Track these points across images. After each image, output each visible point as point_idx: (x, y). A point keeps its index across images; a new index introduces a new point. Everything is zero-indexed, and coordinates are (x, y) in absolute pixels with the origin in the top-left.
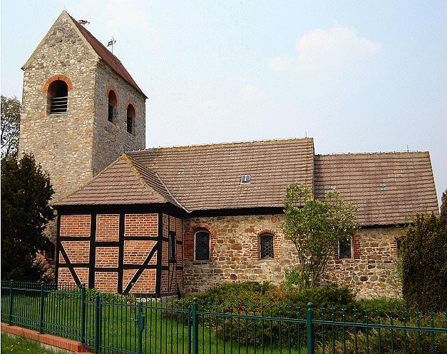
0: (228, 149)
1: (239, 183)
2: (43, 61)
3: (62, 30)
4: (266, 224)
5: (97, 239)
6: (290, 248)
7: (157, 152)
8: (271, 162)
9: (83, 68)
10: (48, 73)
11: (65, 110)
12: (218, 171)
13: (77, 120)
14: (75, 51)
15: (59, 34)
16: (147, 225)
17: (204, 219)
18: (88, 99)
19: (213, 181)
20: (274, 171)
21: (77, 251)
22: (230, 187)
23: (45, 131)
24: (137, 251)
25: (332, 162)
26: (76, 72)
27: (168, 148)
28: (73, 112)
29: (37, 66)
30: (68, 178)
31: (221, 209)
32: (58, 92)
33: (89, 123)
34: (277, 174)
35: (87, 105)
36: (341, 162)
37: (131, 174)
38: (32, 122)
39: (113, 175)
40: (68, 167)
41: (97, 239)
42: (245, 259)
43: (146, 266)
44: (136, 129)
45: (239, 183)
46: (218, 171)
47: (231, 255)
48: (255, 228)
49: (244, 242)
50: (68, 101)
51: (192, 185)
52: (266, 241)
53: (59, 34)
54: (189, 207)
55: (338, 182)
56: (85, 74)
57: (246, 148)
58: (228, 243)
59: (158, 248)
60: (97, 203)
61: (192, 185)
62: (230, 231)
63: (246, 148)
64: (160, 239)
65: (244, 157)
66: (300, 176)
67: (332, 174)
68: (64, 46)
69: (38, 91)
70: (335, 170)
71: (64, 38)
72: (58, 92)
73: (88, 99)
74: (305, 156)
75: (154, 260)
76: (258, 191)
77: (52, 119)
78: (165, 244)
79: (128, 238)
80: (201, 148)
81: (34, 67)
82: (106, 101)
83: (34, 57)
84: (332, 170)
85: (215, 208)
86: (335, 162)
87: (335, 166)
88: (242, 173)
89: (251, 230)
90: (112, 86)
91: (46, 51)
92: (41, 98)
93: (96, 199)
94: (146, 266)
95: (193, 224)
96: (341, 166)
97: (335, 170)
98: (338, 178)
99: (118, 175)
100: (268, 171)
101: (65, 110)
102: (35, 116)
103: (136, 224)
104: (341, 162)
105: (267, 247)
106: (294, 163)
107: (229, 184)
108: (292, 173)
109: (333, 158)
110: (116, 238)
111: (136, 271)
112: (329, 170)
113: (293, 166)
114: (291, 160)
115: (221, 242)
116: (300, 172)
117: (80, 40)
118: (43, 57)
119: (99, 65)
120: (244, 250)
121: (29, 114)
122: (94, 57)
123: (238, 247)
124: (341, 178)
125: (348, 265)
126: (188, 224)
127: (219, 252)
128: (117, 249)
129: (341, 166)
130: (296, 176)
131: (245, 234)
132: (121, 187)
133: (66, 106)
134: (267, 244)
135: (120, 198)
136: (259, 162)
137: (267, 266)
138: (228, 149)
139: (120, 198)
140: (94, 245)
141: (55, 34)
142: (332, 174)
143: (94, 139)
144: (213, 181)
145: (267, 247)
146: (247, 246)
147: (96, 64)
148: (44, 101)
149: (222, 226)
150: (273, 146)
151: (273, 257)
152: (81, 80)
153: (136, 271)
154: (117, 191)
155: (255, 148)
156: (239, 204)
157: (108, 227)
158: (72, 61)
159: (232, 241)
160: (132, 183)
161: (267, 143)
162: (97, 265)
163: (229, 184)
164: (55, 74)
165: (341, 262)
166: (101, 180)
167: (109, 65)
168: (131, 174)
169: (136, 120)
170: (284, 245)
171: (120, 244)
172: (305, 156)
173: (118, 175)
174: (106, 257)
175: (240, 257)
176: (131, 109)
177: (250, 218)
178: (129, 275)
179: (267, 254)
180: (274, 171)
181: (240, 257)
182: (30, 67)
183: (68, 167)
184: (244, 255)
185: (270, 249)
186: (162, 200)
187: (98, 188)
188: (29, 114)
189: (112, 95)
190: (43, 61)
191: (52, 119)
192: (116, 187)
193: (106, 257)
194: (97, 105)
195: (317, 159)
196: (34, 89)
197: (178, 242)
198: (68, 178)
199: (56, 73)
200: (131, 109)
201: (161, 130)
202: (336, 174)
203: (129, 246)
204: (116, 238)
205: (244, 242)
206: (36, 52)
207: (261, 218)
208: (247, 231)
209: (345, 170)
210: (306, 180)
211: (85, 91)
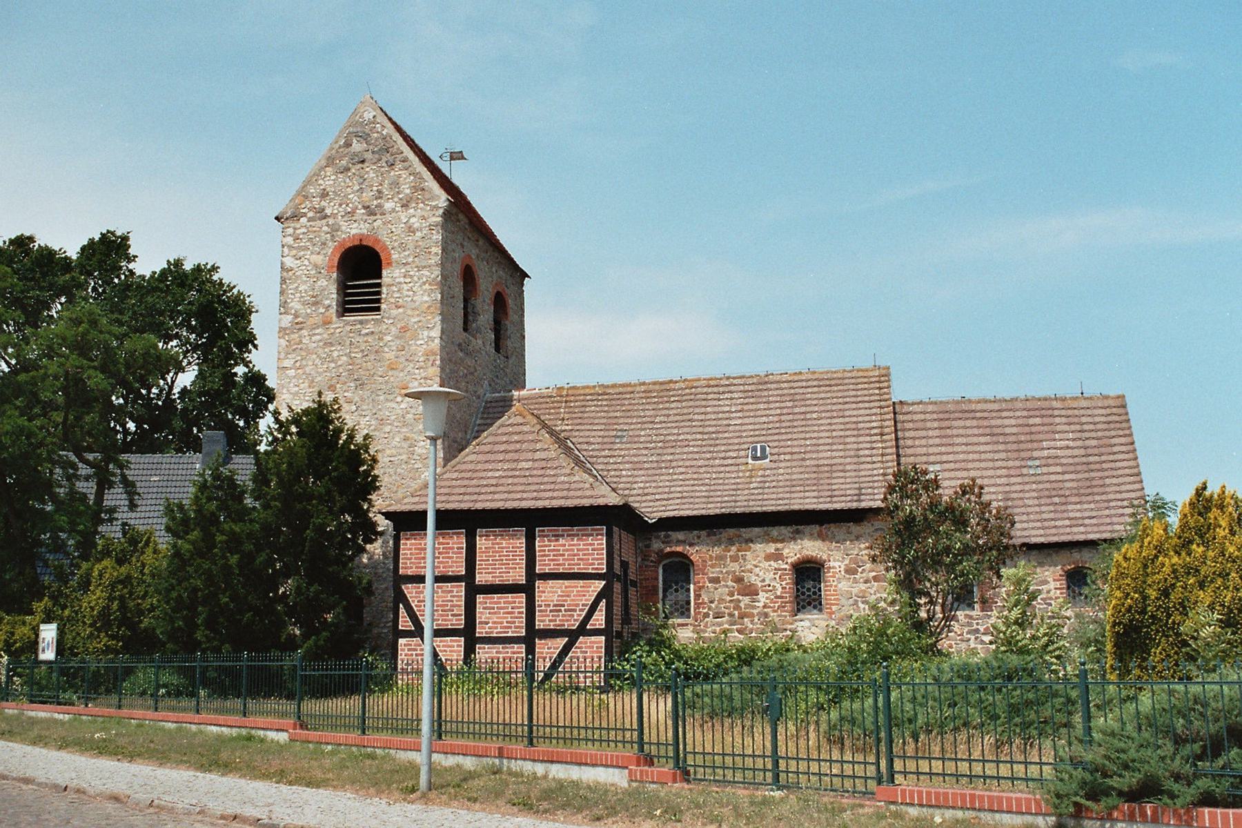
0: (715, 390)
1: (743, 460)
2: (323, 203)
3: (365, 137)
4: (808, 547)
5: (480, 579)
6: (855, 591)
7: (566, 396)
8: (808, 416)
9: (413, 220)
10: (335, 229)
11: (378, 309)
12: (699, 436)
13: (404, 329)
14: (395, 184)
15: (357, 146)
16: (589, 551)
17: (680, 536)
18: (427, 287)
19: (690, 456)
20: (815, 435)
21: (433, 603)
22: (727, 469)
23: (335, 354)
24: (563, 602)
25: (928, 416)
26: (398, 229)
27: (588, 387)
28: (394, 312)
29: (311, 214)
30: (388, 452)
31: (716, 516)
32: (360, 270)
33: (430, 337)
34: (821, 441)
35: (426, 298)
36: (947, 416)
37: (538, 446)
38: (305, 332)
39: (502, 447)
40: (387, 429)
41: (480, 579)
42: (766, 615)
43: (582, 630)
44: (509, 343)
45: (743, 460)
46: (699, 436)
47: (737, 607)
48: (785, 552)
49: (763, 581)
50: (384, 290)
51: (646, 465)
52: (808, 575)
53: (357, 146)
54: (652, 511)
55: (945, 458)
56: (418, 234)
57: (753, 387)
58: (730, 583)
59: (604, 594)
60: (479, 506)
61: (646, 465)
62: (735, 559)
63: (753, 387)
64: (608, 576)
65: (751, 407)
66: (868, 445)
67: (931, 442)
68: (370, 172)
69: (316, 266)
70: (936, 433)
71: (368, 156)
72: (360, 270)
73: (427, 287)
74: (877, 404)
75: (599, 620)
76: (787, 477)
77: (348, 328)
78: (617, 587)
79: (546, 577)
80: (657, 387)
81: (305, 215)
82: (458, 290)
83: (303, 194)
84: (931, 433)
85: (704, 512)
86: (935, 416)
87: (936, 424)
88: (750, 439)
89: (777, 556)
90: (469, 256)
91: (329, 180)
92: (323, 283)
93: (475, 497)
94: (582, 630)
95: (656, 545)
96: (946, 424)
97: (936, 433)
98: (943, 449)
99: (512, 447)
100: (803, 435)
101: (378, 309)
102: (311, 321)
103: (556, 549)
104: (947, 416)
105: (809, 590)
106: (854, 419)
107: (726, 462)
108: (853, 439)
109: (930, 408)
110: (519, 576)
111: (562, 642)
112: (923, 433)
113: (854, 426)
114: (847, 413)
115: (715, 580)
116: (868, 439)
117: (405, 160)
118: (324, 195)
119: (447, 215)
120: (762, 598)
121: (296, 316)
122: (438, 197)
123: (751, 591)
124: (950, 449)
125: (969, 624)
126: (648, 546)
127: (712, 602)
128: (521, 598)
129: (946, 424)
130: (861, 446)
131: (766, 565)
132: (523, 473)
133: (378, 301)
134: (809, 584)
135: (525, 495)
136: (783, 418)
137: (810, 629)
138: (715, 390)
139: (525, 495)
140: (473, 590)
141: (348, 145)
142: (931, 442)
143: (442, 369)
144: (690, 456)
145: (809, 590)
146: (768, 588)
147: (441, 211)
148: (329, 289)
149: (717, 551)
150: (810, 383)
151: (820, 610)
152: (411, 246)
153: (562, 642)
154: (516, 481)
155: (773, 386)
156: (751, 503)
157: (501, 556)
158: (388, 206)
159: (739, 580)
160: (543, 464)
161: (796, 378)
162: (480, 631)
163: (726, 462)
164: (353, 232)
165: (954, 618)
166: (481, 457)
167: (462, 216)
168: (538, 446)
169: (508, 324)
170: (844, 586)
171: (527, 589)
172: (877, 404)
173: (512, 447)
174: (500, 616)
175: (755, 612)
176: (500, 302)
177: (775, 532)
178: (548, 650)
179: (809, 604)
180: (815, 435)
181: (755, 612)
182: (296, 216)
183: (387, 429)
184: (764, 607)
185: (815, 593)
186: (613, 500)
187: (475, 475)
188: (296, 316)
189: (468, 276)
190: (323, 203)
191: (348, 328)
192: (510, 473)
193: (500, 616)
194: (446, 299)
195: (896, 409)
196: (306, 262)
197: (634, 584)
198: (388, 452)
199: (354, 230)
200: (500, 302)
201: (560, 345)
202: (937, 441)
203: (547, 593)
204: (519, 576)
205: (763, 581)
206: (308, 182)
207: (798, 532)
208: (768, 558)
209: (955, 432)
210: (883, 455)
211: (419, 268)
